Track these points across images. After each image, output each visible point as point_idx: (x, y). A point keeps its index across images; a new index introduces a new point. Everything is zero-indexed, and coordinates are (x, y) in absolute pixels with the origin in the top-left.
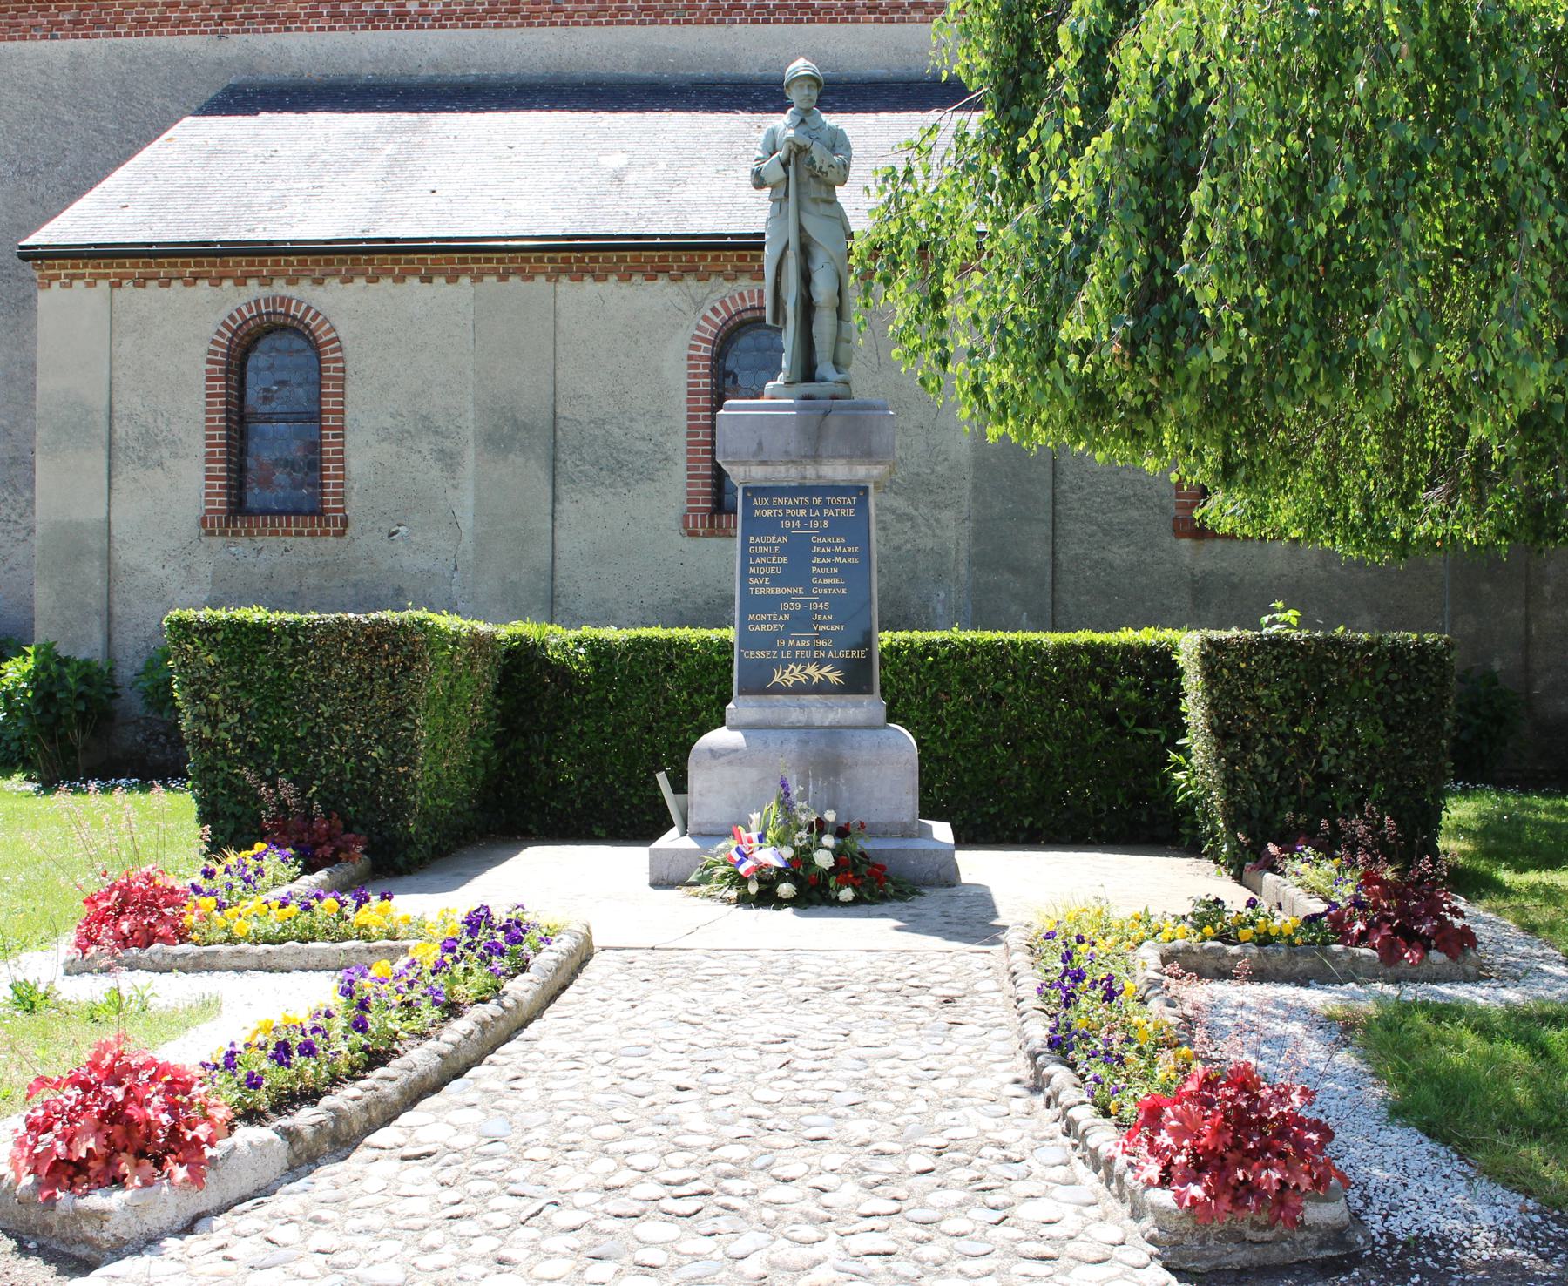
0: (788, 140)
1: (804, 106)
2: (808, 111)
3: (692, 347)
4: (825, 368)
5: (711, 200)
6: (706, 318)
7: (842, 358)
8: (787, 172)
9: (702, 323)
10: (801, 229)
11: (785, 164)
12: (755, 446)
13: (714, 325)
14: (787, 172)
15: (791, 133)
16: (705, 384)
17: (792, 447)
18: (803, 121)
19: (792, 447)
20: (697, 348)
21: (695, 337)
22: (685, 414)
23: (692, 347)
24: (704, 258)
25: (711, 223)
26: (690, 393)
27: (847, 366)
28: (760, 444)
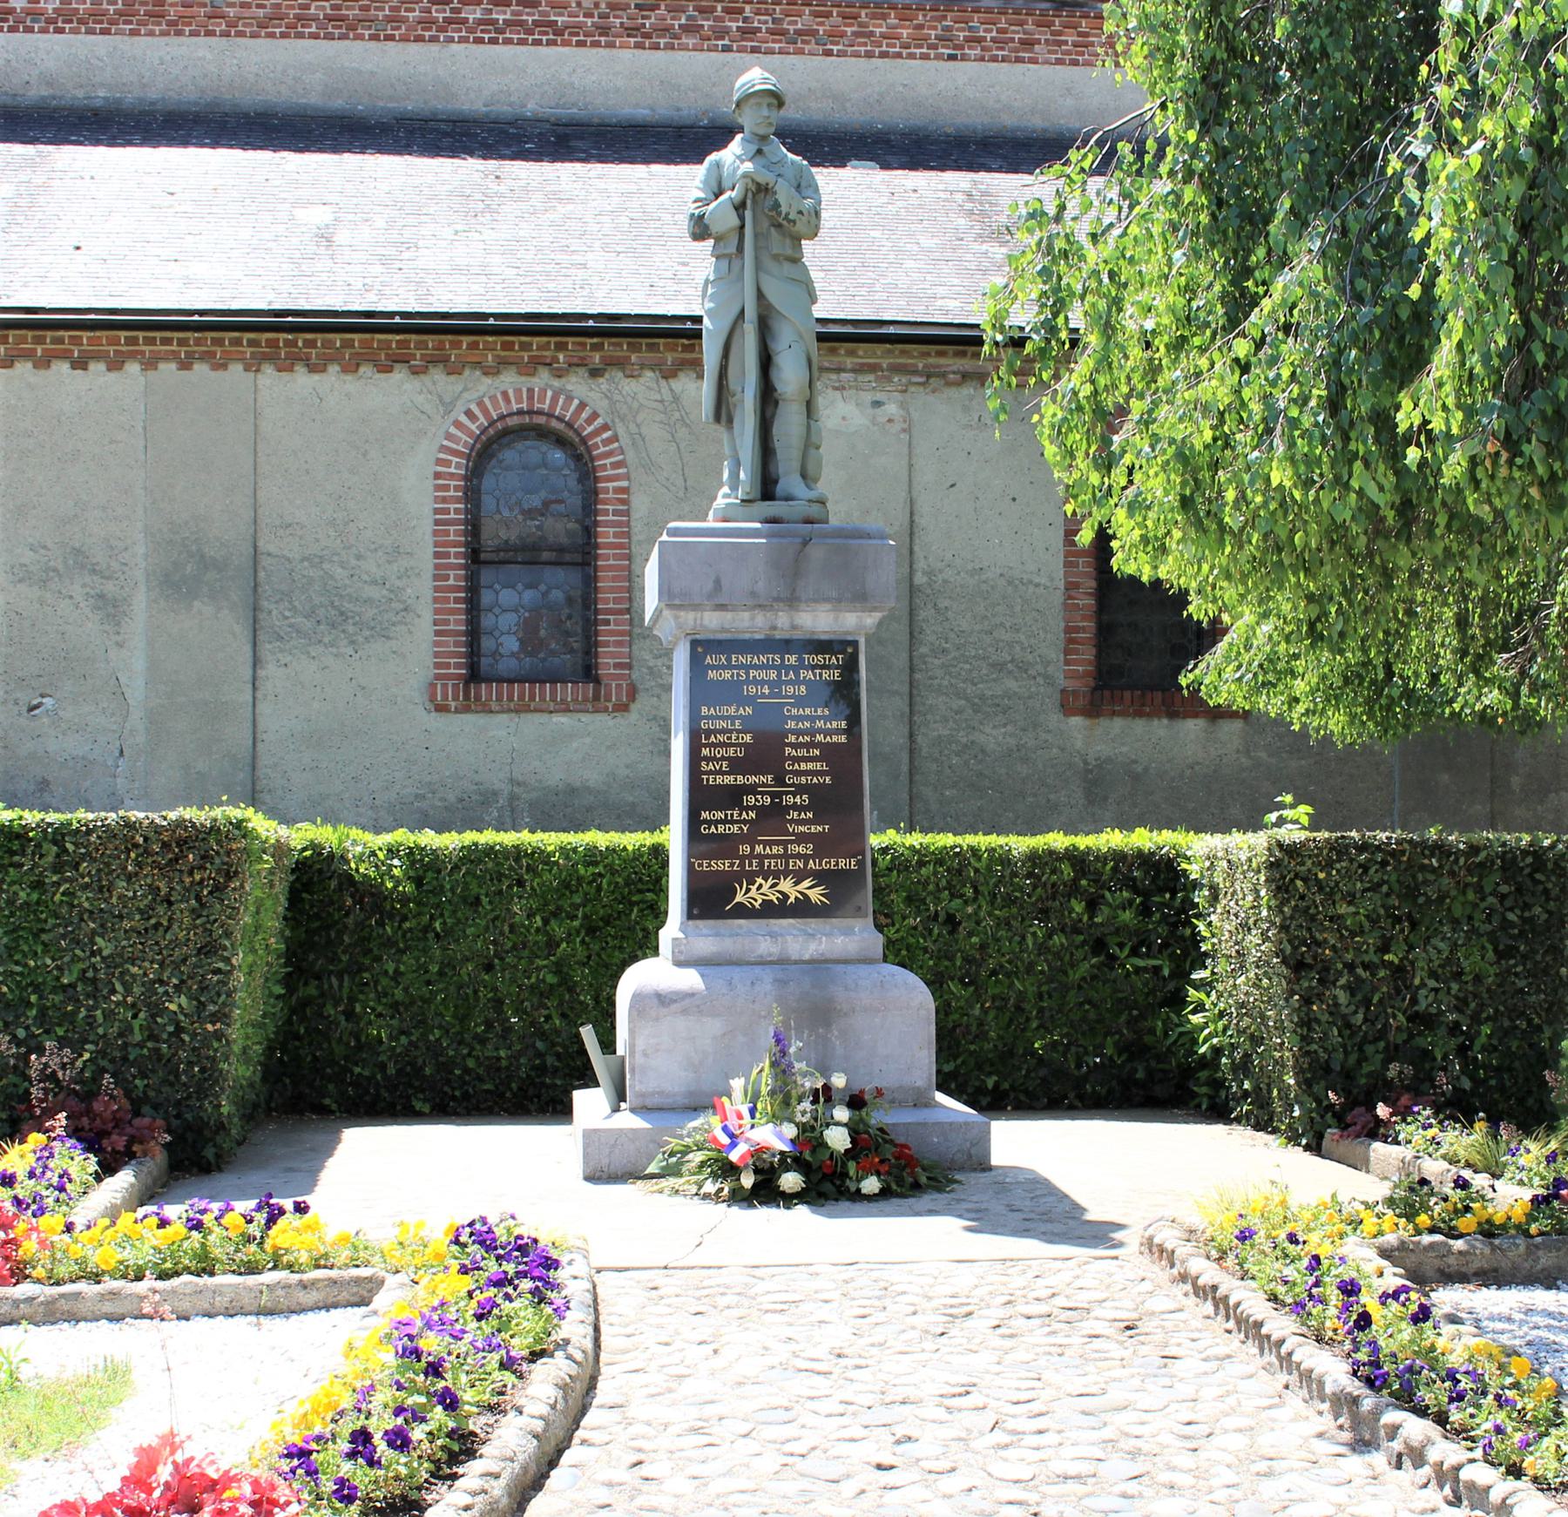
0: (745, 175)
4: (790, 481)
8: (742, 218)
10: (760, 295)
14: (742, 218)
18: (759, 152)
27: (816, 480)
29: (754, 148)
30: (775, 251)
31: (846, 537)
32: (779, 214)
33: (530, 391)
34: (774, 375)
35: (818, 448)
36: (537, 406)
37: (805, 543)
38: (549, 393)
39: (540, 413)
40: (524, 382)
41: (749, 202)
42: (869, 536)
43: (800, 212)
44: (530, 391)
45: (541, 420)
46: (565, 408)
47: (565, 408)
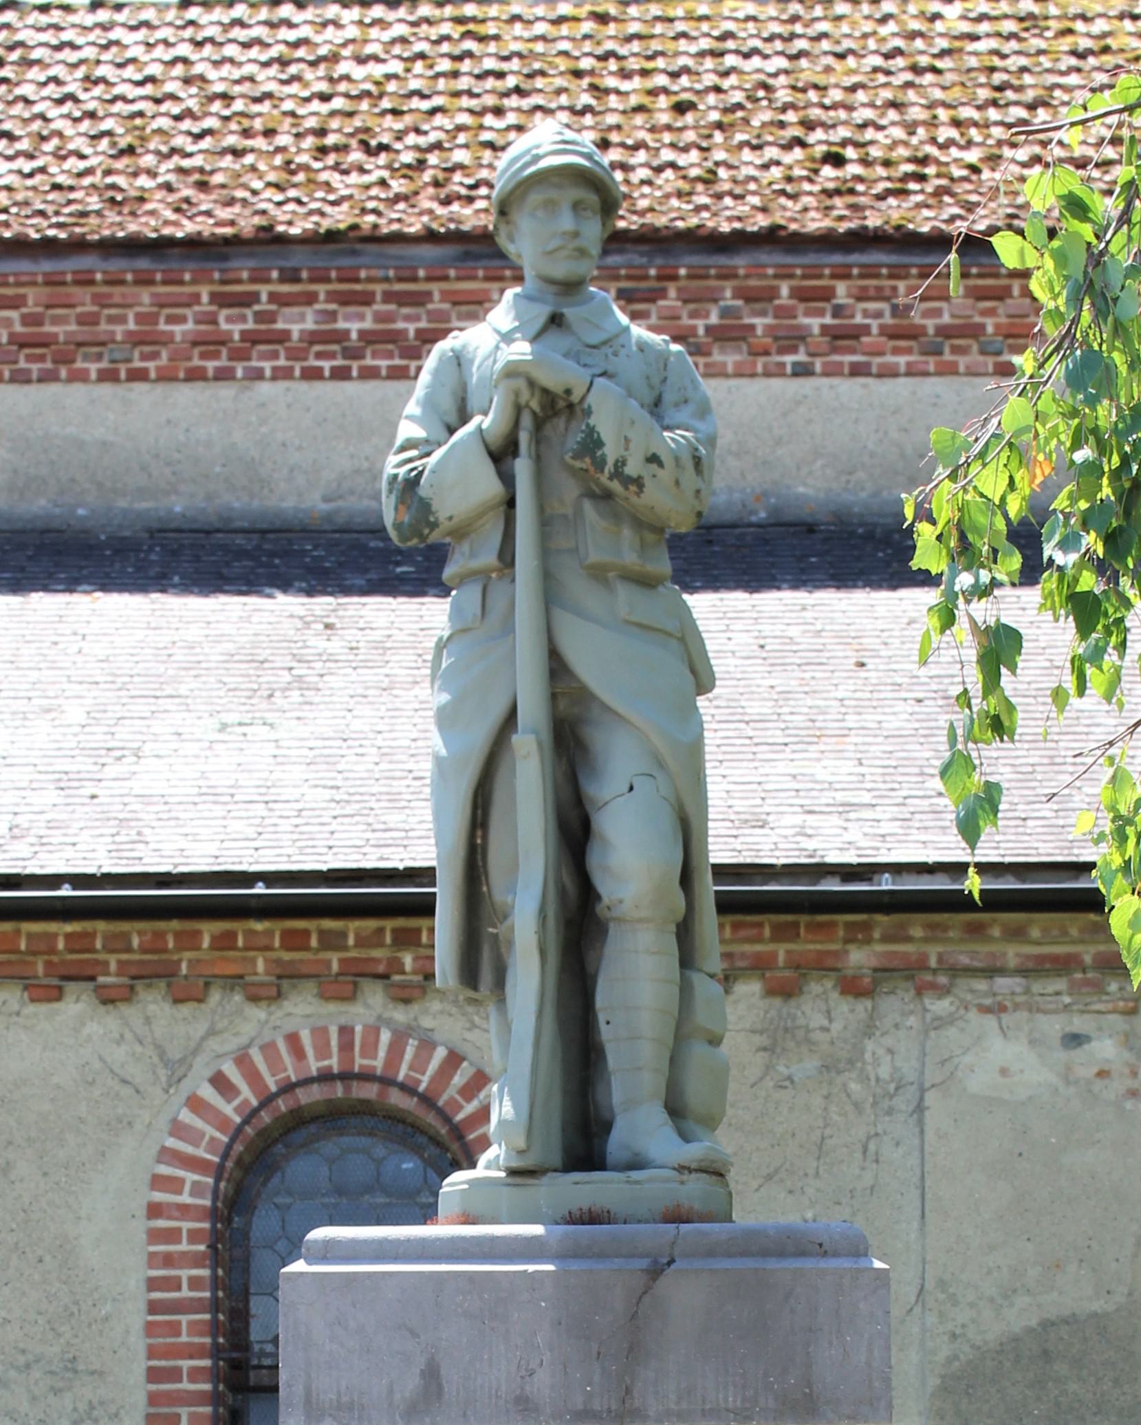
0: (512, 371)
1: (561, 270)
2: (570, 288)
3: (158, 1182)
4: (639, 1124)
5: (211, 794)
6: (196, 1104)
7: (695, 1093)
8: (508, 479)
9: (186, 1116)
10: (557, 667)
11: (501, 454)
12: (411, 1383)
13: (221, 1123)
14: (508, 479)
15: (522, 350)
16: (195, 1283)
17: (543, 1384)
18: (556, 320)
19: (543, 1384)
20: (174, 1185)
21: (167, 1155)
22: (140, 1365)
23: (158, 1182)
24: (189, 941)
25: (212, 848)
26: (154, 1307)
27: (711, 1122)
28: (432, 1374)
29: (541, 312)
30: (594, 557)
31: (765, 1253)
32: (600, 464)
33: (346, 1032)
34: (594, 861)
35: (715, 1041)
36: (359, 1062)
37: (656, 1272)
38: (385, 1037)
39: (366, 1076)
40: (334, 1014)
41: (524, 438)
42: (822, 1250)
43: (654, 459)
44: (346, 1032)
45: (369, 1091)
46: (419, 1064)
47: (419, 1064)
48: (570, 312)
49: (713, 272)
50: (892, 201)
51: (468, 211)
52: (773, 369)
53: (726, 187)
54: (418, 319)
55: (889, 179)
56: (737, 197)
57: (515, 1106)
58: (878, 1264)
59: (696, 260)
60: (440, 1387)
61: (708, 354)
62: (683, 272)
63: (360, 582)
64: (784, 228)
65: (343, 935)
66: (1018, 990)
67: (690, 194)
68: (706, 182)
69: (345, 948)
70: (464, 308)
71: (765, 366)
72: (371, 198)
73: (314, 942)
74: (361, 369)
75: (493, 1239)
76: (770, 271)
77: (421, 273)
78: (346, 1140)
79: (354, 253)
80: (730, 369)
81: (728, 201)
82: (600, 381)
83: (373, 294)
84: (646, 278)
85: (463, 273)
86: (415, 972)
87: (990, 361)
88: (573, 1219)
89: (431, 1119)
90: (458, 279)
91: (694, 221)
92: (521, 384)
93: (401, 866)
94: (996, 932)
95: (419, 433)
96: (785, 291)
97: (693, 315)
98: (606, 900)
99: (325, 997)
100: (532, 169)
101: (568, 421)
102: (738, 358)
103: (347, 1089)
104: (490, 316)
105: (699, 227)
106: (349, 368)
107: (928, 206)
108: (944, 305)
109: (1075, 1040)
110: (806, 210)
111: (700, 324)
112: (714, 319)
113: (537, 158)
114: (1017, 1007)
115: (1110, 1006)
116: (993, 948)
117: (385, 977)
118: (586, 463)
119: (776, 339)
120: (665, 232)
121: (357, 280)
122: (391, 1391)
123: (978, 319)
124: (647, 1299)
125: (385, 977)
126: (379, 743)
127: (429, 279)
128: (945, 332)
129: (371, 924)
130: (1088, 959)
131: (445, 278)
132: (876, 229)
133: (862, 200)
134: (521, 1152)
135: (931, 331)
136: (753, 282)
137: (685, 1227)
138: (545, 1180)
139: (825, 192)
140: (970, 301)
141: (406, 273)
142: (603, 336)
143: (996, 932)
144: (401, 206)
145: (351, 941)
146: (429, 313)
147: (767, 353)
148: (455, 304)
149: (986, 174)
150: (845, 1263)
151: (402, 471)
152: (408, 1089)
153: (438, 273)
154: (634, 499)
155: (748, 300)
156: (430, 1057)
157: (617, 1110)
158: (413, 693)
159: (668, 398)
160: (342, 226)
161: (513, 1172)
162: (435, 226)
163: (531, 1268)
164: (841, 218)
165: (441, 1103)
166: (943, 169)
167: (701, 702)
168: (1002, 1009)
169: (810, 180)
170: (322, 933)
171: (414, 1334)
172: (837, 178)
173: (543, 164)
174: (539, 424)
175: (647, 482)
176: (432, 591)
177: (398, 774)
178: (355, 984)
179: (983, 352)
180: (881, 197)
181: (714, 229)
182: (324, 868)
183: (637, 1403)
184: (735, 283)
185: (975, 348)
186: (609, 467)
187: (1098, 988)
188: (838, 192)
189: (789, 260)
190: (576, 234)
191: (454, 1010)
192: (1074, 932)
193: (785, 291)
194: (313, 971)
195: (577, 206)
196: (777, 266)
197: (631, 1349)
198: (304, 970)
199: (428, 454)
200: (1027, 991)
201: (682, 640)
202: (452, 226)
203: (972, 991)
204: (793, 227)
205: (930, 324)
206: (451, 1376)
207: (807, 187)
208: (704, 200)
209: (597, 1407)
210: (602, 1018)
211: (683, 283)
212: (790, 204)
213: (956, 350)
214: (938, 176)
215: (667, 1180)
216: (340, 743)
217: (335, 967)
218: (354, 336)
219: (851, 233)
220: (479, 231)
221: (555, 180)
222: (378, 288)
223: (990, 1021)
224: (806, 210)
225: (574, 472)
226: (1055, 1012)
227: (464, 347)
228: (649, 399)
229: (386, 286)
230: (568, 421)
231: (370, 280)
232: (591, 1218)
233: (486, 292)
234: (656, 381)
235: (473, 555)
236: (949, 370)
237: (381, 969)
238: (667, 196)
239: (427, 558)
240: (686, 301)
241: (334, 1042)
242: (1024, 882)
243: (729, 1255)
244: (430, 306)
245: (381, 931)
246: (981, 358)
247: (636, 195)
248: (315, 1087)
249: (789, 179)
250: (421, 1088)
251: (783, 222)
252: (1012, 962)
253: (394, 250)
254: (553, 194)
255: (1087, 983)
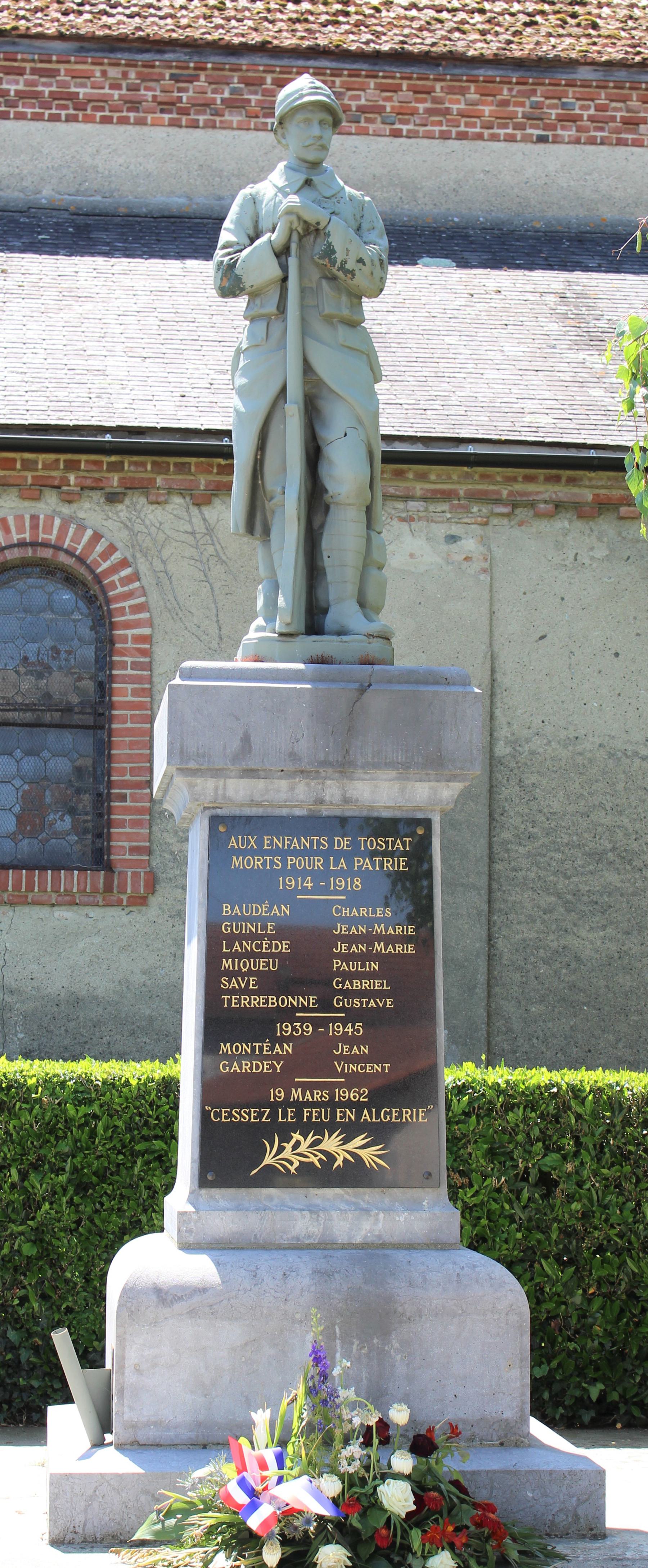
0: (289, 212)
4: (343, 611)
7: (371, 596)
8: (284, 268)
10: (307, 368)
14: (284, 268)
18: (308, 183)
27: (378, 610)
28: (246, 740)
29: (301, 178)
30: (327, 311)
31: (418, 682)
32: (333, 262)
33: (34, 518)
34: (324, 471)
35: (380, 568)
36: (42, 536)
37: (362, 690)
38: (57, 522)
39: (45, 545)
40: (28, 508)
41: (294, 247)
42: (447, 682)
43: (360, 261)
44: (34, 518)
45: (47, 553)
46: (76, 539)
47: (76, 539)
48: (315, 179)
49: (227, 67)
50: (330, 28)
51: (80, 20)
52: (260, 126)
53: (232, 13)
54: (51, 85)
55: (327, 13)
56: (239, 20)
57: (286, 600)
58: (477, 690)
59: (217, 59)
60: (250, 747)
61: (223, 115)
62: (209, 66)
63: (18, 244)
64: (270, 43)
65: (36, 462)
66: (421, 509)
67: (211, 17)
68: (220, 9)
69: (37, 470)
70: (78, 80)
71: (255, 124)
72: (20, 9)
73: (18, 466)
74: (16, 113)
75: (277, 670)
76: (261, 68)
77: (54, 58)
78: (31, 581)
79: (14, 43)
80: (235, 125)
81: (234, 23)
82: (334, 217)
83: (25, 68)
84: (188, 68)
85: (79, 59)
86: (75, 486)
87: (388, 128)
88: (313, 661)
89: (82, 570)
90: (76, 63)
91: (216, 35)
92: (294, 218)
93: (71, 424)
94: (411, 476)
95: (232, 238)
96: (269, 80)
97: (214, 91)
98: (331, 493)
99: (23, 497)
100: (300, 102)
101: (315, 238)
102: (240, 118)
103: (35, 552)
104: (270, 177)
105: (220, 39)
106: (9, 112)
107: (352, 33)
108: (362, 93)
109: (452, 539)
110: (280, 31)
111: (218, 97)
112: (226, 95)
113: (302, 96)
114: (420, 519)
115: (473, 520)
116: (408, 484)
117: (59, 487)
118: (326, 262)
119: (263, 108)
120: (200, 42)
121: (16, 60)
122: (225, 748)
123: (381, 103)
124: (358, 704)
125: (59, 487)
126: (45, 346)
127: (58, 62)
128: (362, 109)
129: (52, 457)
130: (462, 493)
131: (69, 62)
132: (324, 46)
133: (314, 27)
134: (288, 624)
135: (354, 109)
136: (250, 74)
137: (376, 667)
138: (298, 639)
139: (290, 19)
140: (378, 92)
141: (45, 58)
142: (333, 192)
143: (411, 476)
144: (39, 15)
145: (40, 466)
146: (57, 81)
147: (257, 117)
148: (73, 77)
149: (384, 13)
150: (460, 689)
151: (226, 259)
152: (70, 553)
153: (64, 59)
154: (349, 281)
155: (247, 84)
156: (83, 535)
157: (332, 603)
158: (62, 315)
159: (365, 226)
160: (8, 27)
161: (281, 635)
162: (63, 30)
163: (298, 686)
164: (302, 38)
165: (88, 562)
166: (359, 9)
167: (377, 386)
168: (412, 519)
169: (281, 12)
170: (23, 460)
171: (237, 719)
172: (296, 12)
173: (306, 99)
174: (301, 238)
175: (357, 272)
176: (62, 252)
177: (59, 366)
178: (41, 491)
179: (383, 123)
180: (324, 25)
181: (229, 41)
182: (27, 423)
183: (352, 758)
184: (239, 74)
185: (379, 119)
186: (338, 264)
187: (467, 510)
188: (298, 21)
189: (273, 62)
190: (321, 138)
191: (97, 508)
192: (455, 477)
193: (269, 80)
194: (18, 482)
195: (321, 122)
196: (265, 65)
197: (349, 730)
198: (12, 481)
199: (241, 251)
200: (426, 510)
201: (368, 355)
202: (74, 31)
203: (395, 509)
204: (276, 42)
205: (354, 104)
206: (256, 741)
207: (279, 16)
208: (219, 21)
209: (331, 759)
210: (325, 554)
211: (208, 72)
212: (270, 26)
213: (368, 120)
214: (356, 13)
215: (362, 641)
216: (22, 345)
217: (30, 481)
218: (12, 93)
219: (309, 48)
220: (90, 35)
221: (310, 108)
222: (28, 66)
223: (405, 526)
224: (280, 31)
225: (317, 265)
226: (442, 522)
227: (257, 193)
228: (355, 227)
229: (32, 65)
230: (315, 238)
231: (23, 60)
232: (322, 660)
233: (93, 71)
234: (358, 217)
235: (262, 306)
236: (364, 132)
237: (56, 483)
238: (197, 17)
239: (56, 231)
240: (210, 83)
241: (27, 524)
242: (428, 447)
243: (399, 683)
244: (58, 78)
245: (57, 460)
246: (382, 126)
247: (179, 15)
248: (16, 549)
249: (269, 10)
250: (77, 553)
251: (269, 39)
252: (419, 493)
253: (38, 43)
254: (309, 116)
255: (460, 506)
